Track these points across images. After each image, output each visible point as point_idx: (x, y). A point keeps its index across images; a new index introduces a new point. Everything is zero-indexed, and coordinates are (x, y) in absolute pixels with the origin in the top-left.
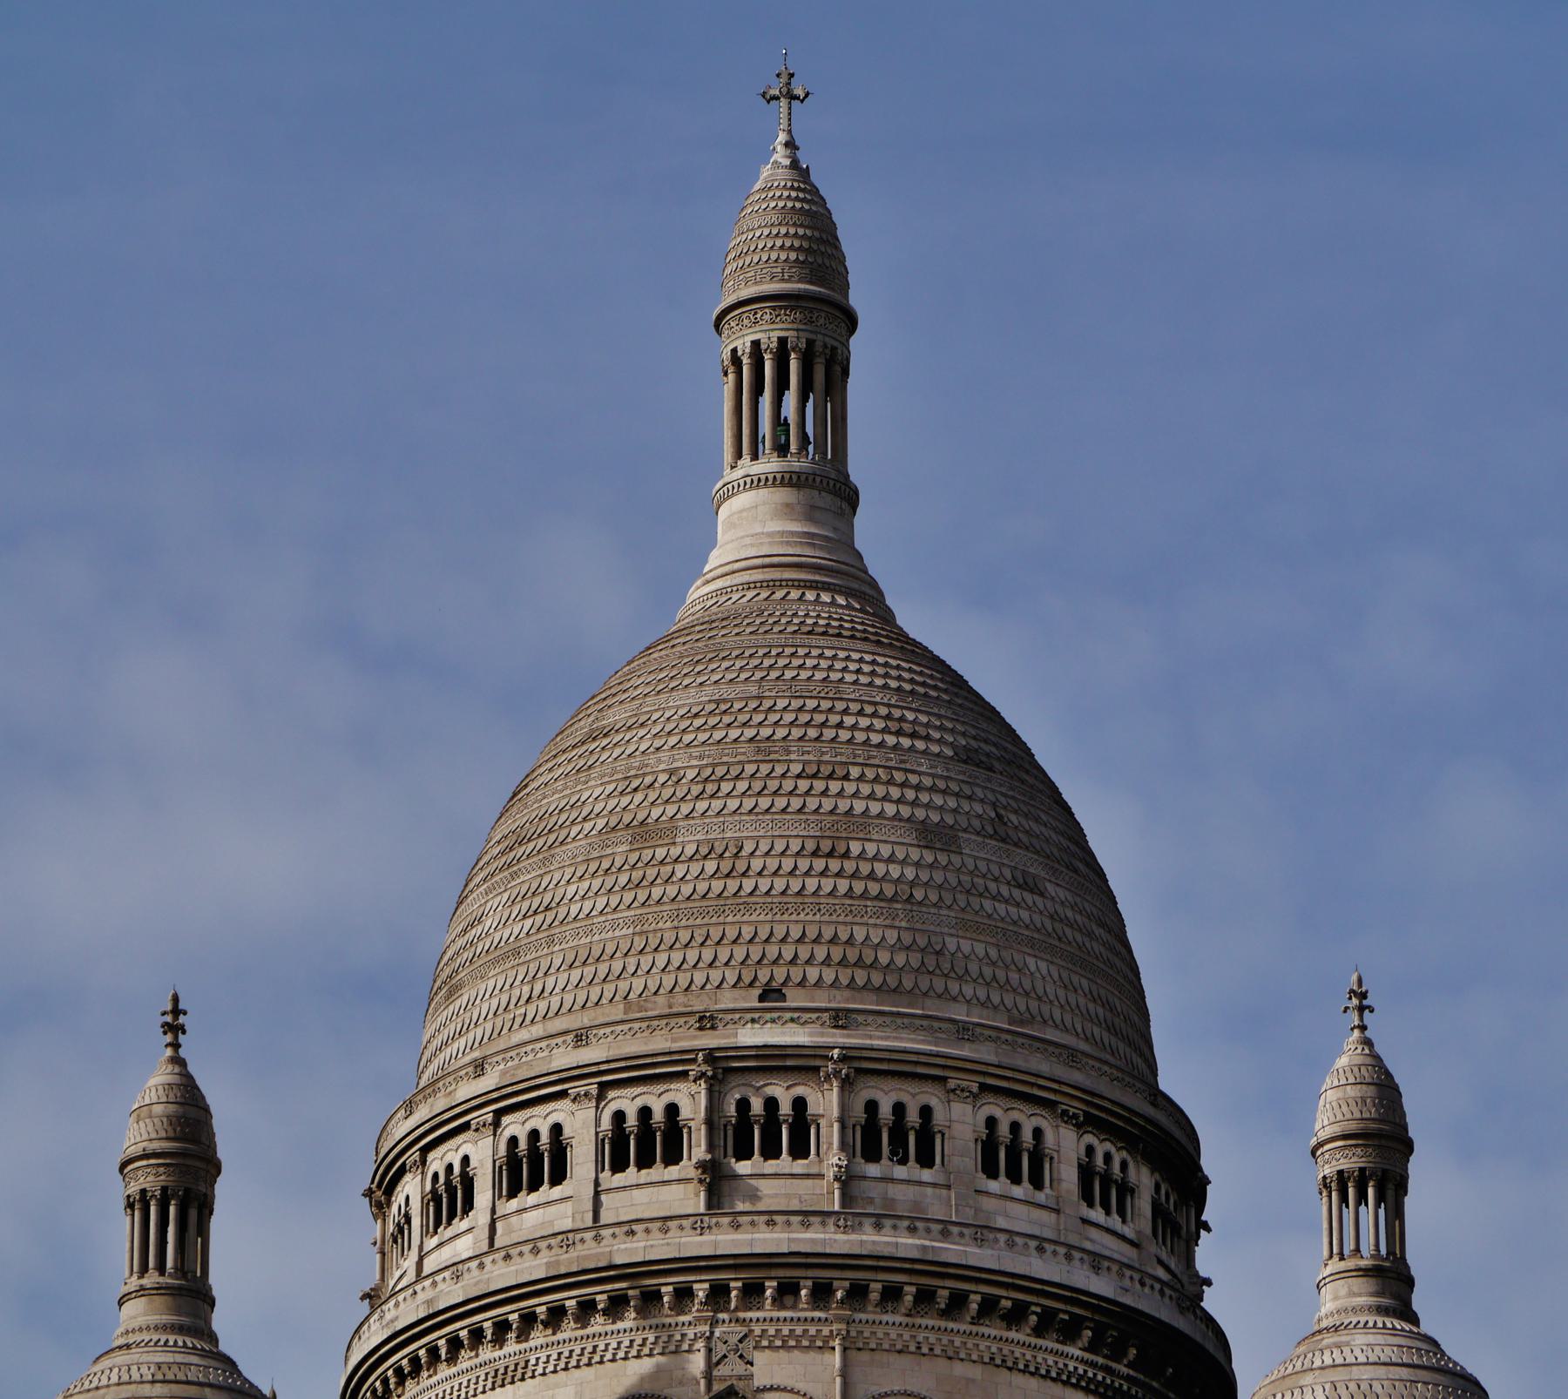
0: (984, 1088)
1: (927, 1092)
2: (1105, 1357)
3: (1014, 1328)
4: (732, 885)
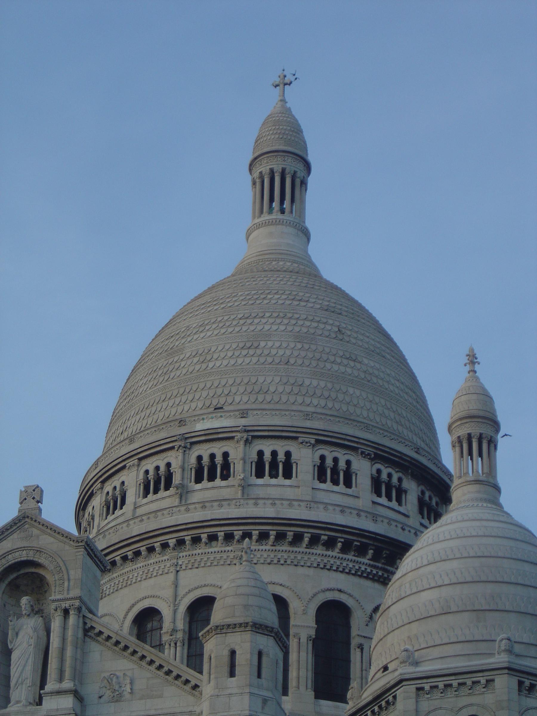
0: (318, 442)
1: (289, 445)
2: (383, 564)
3: (330, 550)
4: (204, 366)
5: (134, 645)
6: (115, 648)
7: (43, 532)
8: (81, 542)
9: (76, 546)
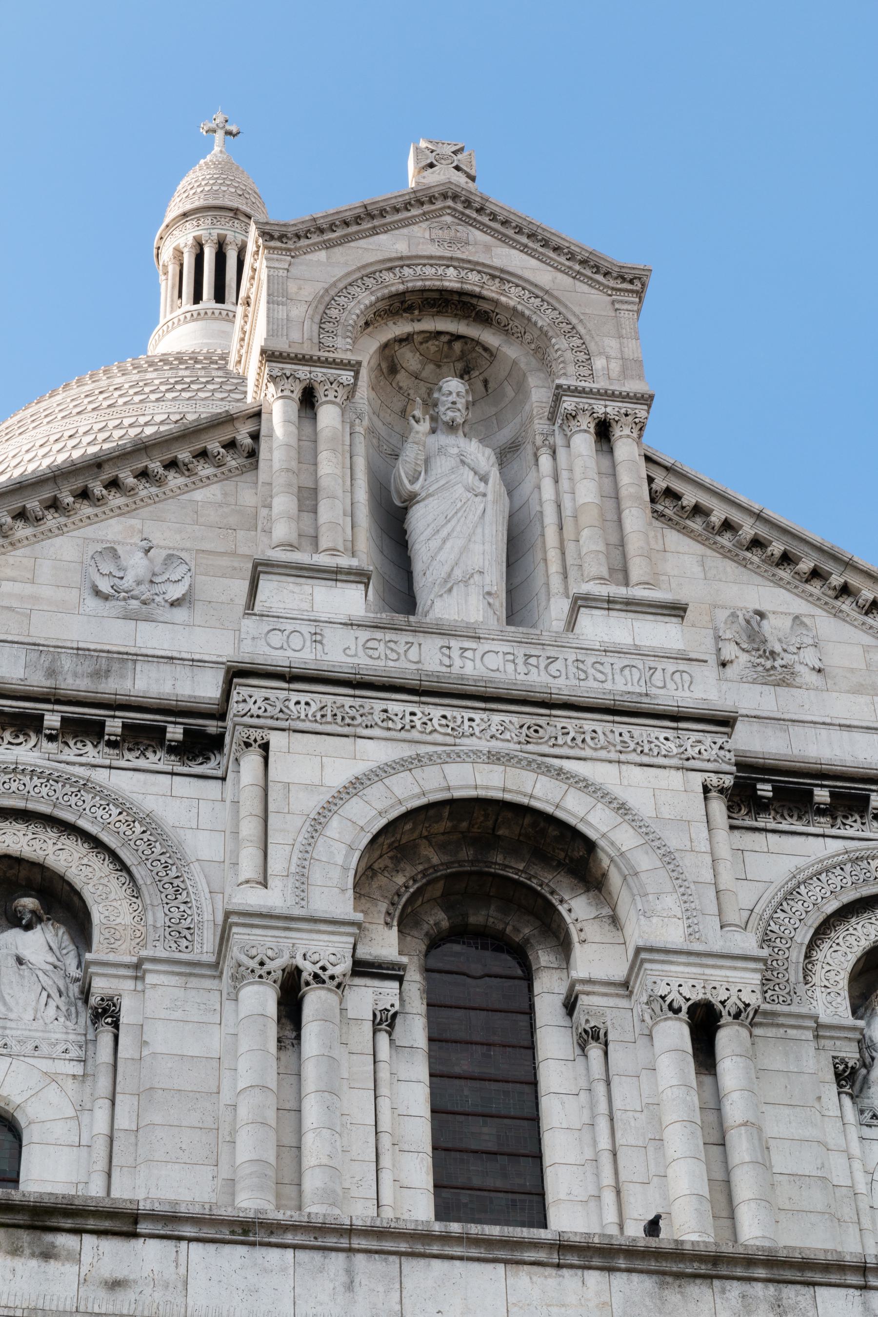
5: (814, 554)
6: (748, 555)
7: (504, 239)
8: (631, 282)
9: (613, 289)
